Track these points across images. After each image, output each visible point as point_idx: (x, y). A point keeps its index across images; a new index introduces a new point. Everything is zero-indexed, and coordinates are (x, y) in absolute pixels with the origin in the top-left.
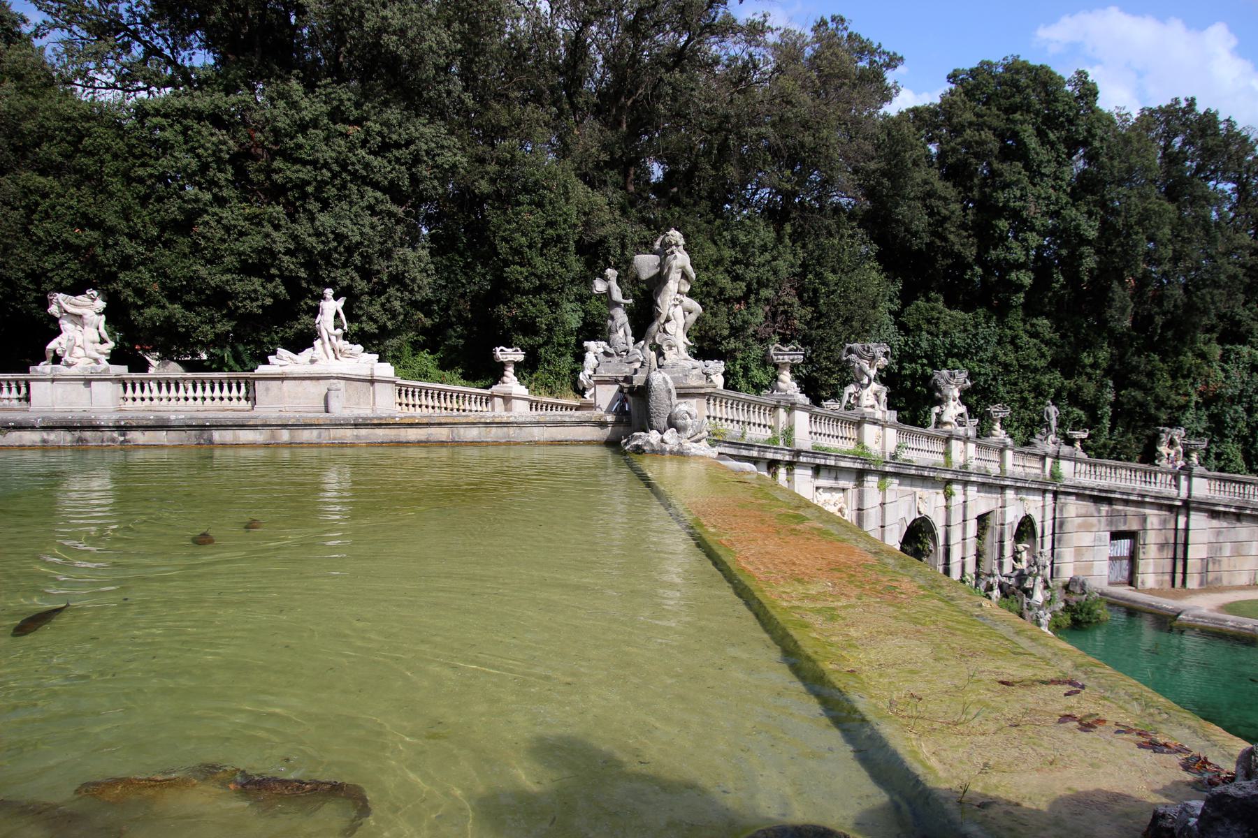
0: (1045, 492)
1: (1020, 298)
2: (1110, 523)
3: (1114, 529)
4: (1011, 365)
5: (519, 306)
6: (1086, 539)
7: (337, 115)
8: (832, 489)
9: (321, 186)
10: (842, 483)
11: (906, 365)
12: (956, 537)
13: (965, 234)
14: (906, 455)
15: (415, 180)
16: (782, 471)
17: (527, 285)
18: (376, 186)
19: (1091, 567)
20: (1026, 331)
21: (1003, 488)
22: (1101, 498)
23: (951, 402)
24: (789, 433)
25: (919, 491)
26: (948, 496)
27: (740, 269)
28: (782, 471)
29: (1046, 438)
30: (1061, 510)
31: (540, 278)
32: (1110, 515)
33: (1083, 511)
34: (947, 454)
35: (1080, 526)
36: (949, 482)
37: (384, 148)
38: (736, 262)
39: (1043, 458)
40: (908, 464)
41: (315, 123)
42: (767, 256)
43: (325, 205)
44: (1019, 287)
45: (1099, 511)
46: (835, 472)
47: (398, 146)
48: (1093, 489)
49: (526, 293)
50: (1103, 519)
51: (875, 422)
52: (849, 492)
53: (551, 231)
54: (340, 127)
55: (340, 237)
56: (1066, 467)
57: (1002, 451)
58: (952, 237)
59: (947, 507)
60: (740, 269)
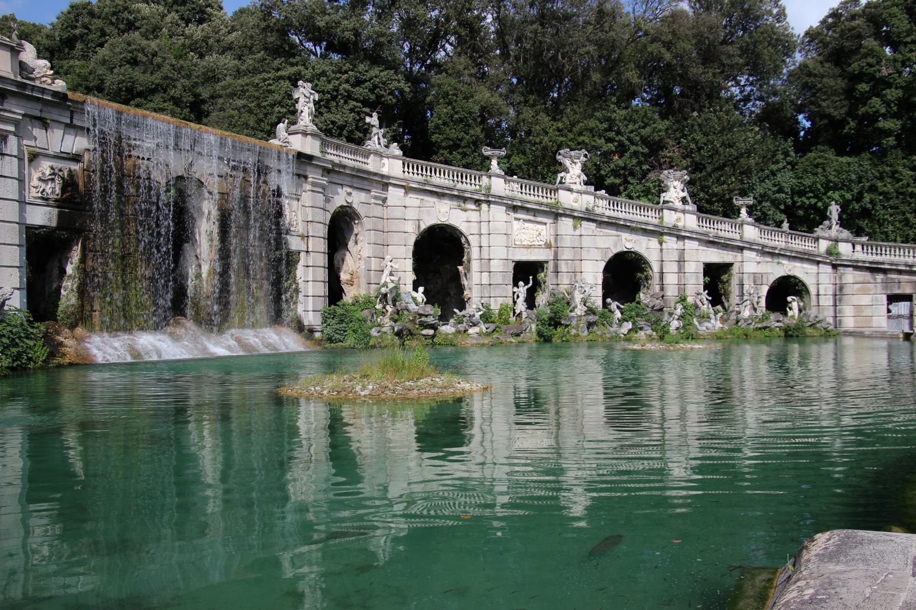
0: (818, 263)
1: (891, 141)
2: (886, 288)
3: (889, 292)
4: (888, 193)
5: (442, 155)
6: (865, 300)
7: (340, 71)
8: (530, 221)
9: (328, 101)
10: (539, 219)
11: (796, 199)
13: (837, 99)
14: (598, 211)
15: (379, 97)
16: (484, 206)
17: (444, 144)
18: (356, 100)
19: (871, 321)
20: (905, 166)
21: (741, 249)
22: (874, 269)
23: (672, 189)
24: (489, 188)
25: (625, 235)
26: (661, 244)
27: (612, 134)
28: (484, 206)
29: (830, 228)
30: (841, 278)
31: (452, 140)
32: (885, 283)
33: (860, 279)
34: (661, 218)
35: (859, 290)
36: (662, 234)
37: (358, 83)
38: (606, 130)
39: (817, 239)
40: (602, 215)
41: (323, 73)
42: (637, 126)
43: (329, 111)
44: (888, 133)
45: (875, 279)
46: (535, 212)
47: (366, 81)
48: (864, 262)
49: (445, 148)
50: (879, 286)
53: (456, 116)
54: (338, 75)
55: (333, 123)
56: (844, 249)
57: (742, 225)
58: (824, 104)
59: (661, 250)
60: (612, 134)
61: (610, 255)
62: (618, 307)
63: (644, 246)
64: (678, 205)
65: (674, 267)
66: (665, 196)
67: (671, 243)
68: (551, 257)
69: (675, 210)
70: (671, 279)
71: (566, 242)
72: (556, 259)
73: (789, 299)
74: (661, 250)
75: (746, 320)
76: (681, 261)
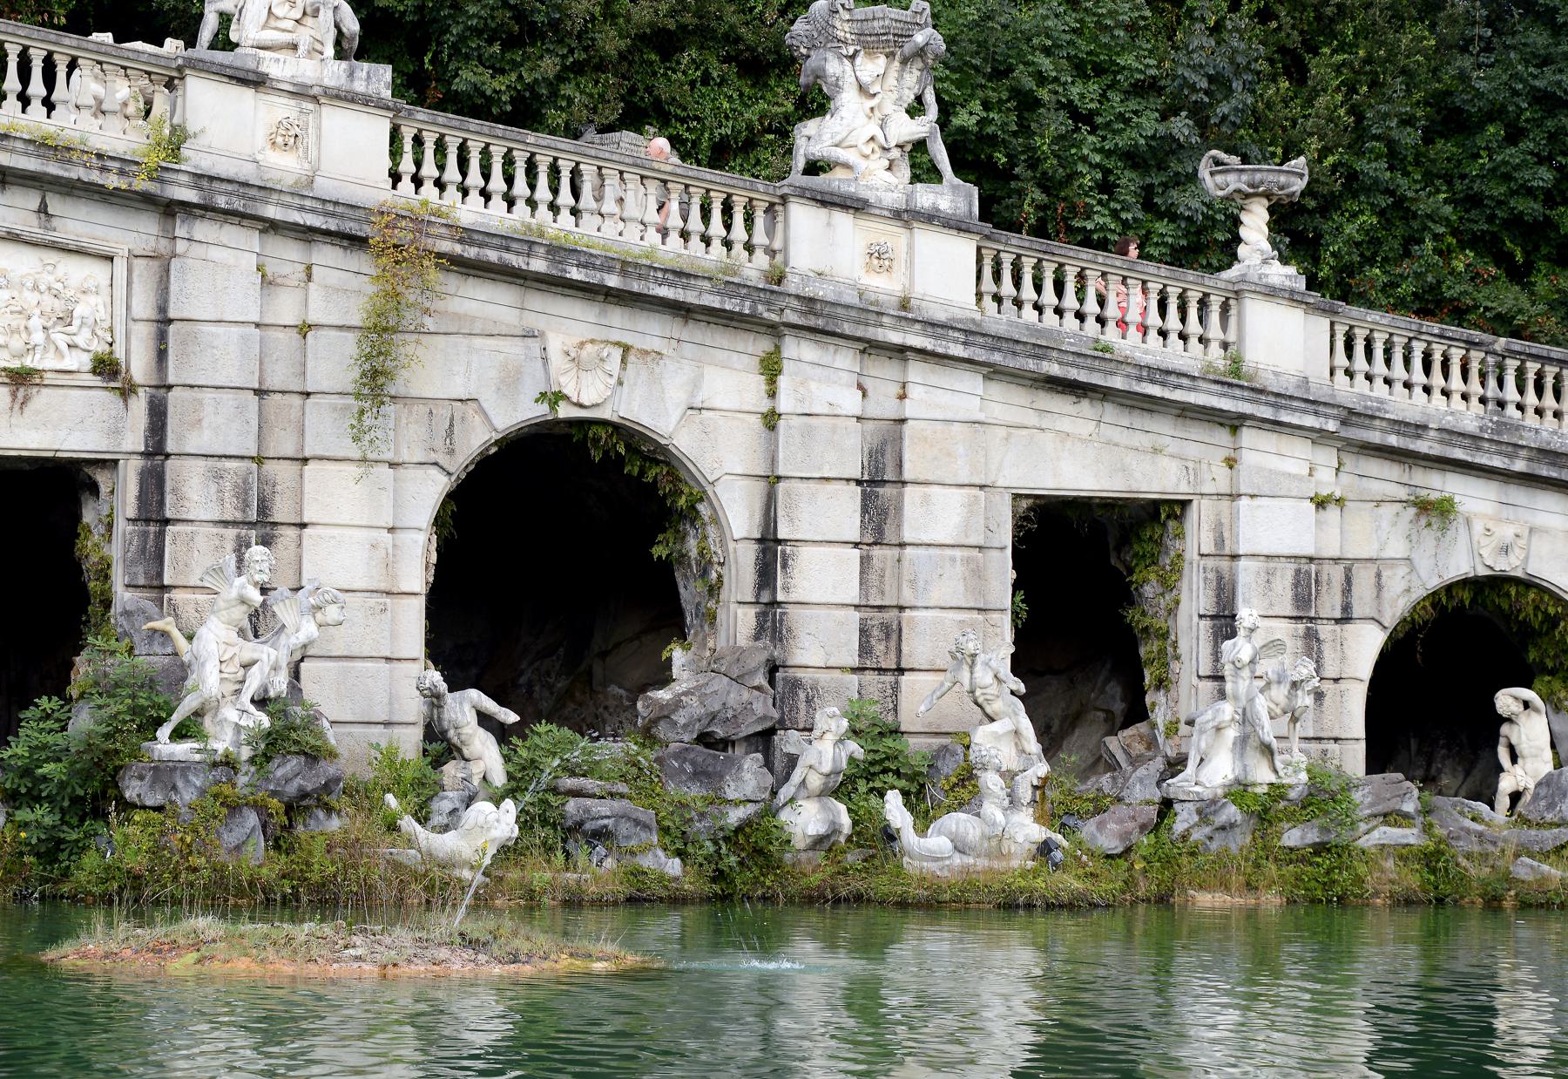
12: (824, 517)
51: (256, 81)
52: (120, 266)
59: (771, 420)
61: (476, 440)
62: (485, 720)
63: (675, 394)
64: (885, 182)
65: (842, 512)
66: (813, 138)
67: (821, 381)
68: (134, 438)
69: (856, 206)
70: (823, 579)
71: (217, 358)
72: (156, 450)
73: (1506, 700)
74: (771, 420)
75: (1206, 810)
76: (879, 484)
